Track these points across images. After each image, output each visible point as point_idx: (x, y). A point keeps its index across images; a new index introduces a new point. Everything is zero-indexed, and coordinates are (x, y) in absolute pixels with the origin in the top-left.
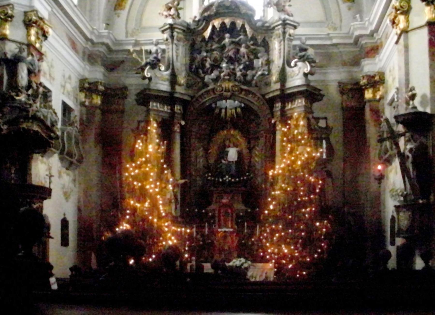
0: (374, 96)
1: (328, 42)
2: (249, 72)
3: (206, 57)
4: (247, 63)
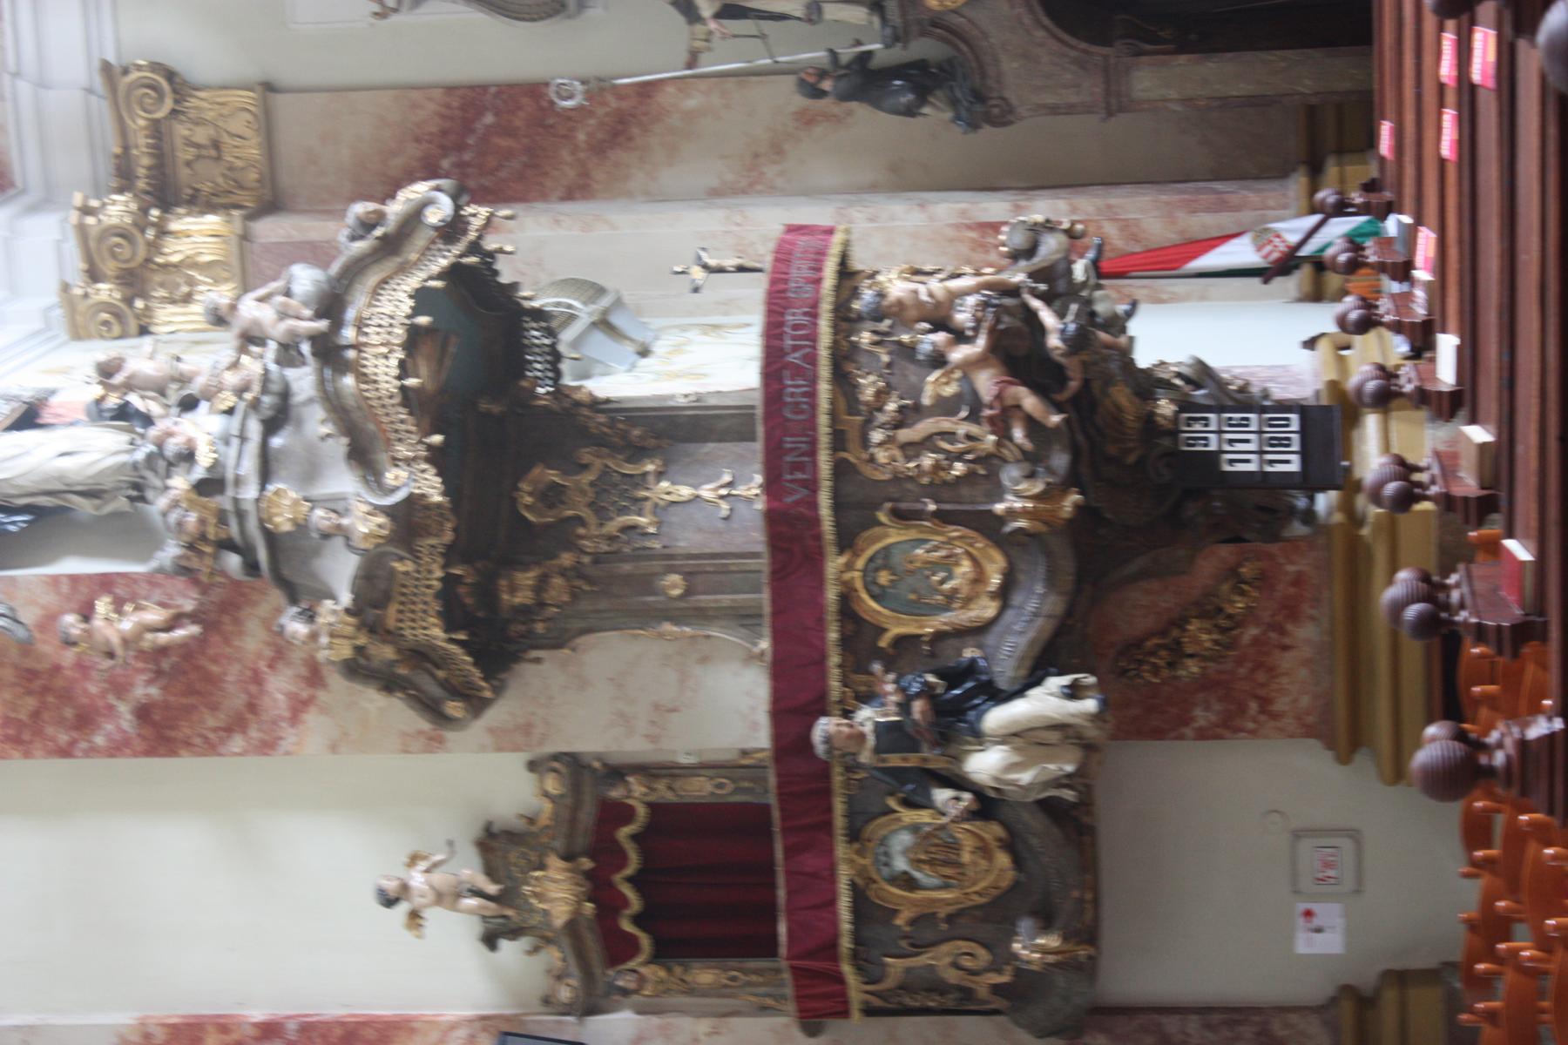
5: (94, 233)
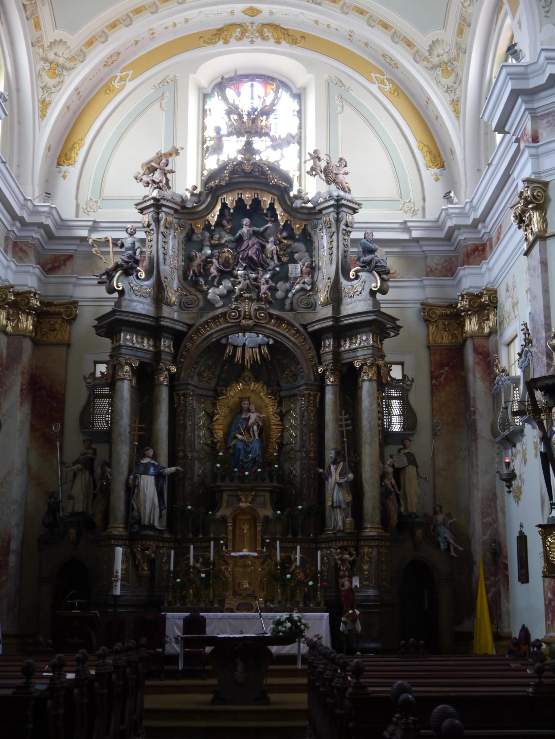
0: (481, 328)
1: (405, 236)
2: (281, 285)
3: (211, 256)
4: (278, 269)
5: (28, 296)
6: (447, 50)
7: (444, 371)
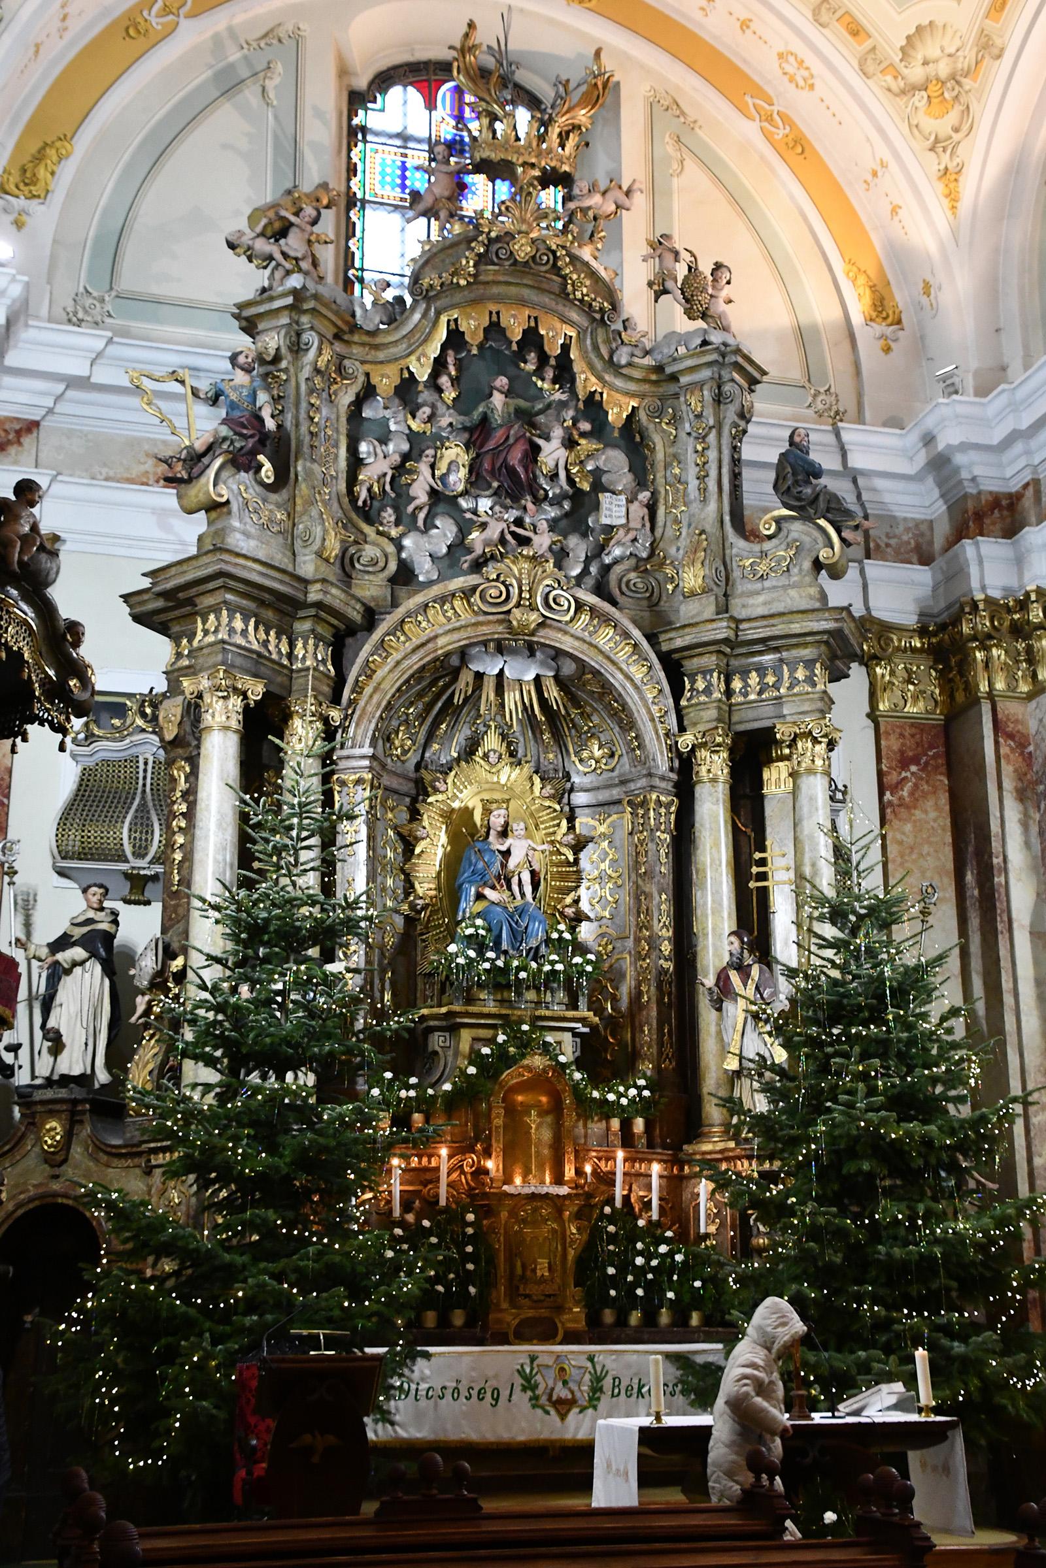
6: (952, 50)
7: (908, 774)
